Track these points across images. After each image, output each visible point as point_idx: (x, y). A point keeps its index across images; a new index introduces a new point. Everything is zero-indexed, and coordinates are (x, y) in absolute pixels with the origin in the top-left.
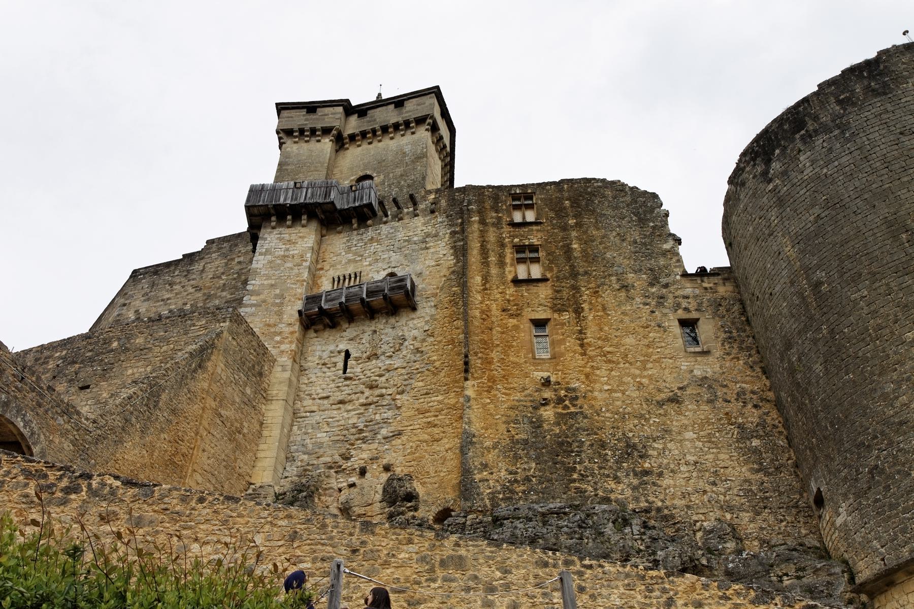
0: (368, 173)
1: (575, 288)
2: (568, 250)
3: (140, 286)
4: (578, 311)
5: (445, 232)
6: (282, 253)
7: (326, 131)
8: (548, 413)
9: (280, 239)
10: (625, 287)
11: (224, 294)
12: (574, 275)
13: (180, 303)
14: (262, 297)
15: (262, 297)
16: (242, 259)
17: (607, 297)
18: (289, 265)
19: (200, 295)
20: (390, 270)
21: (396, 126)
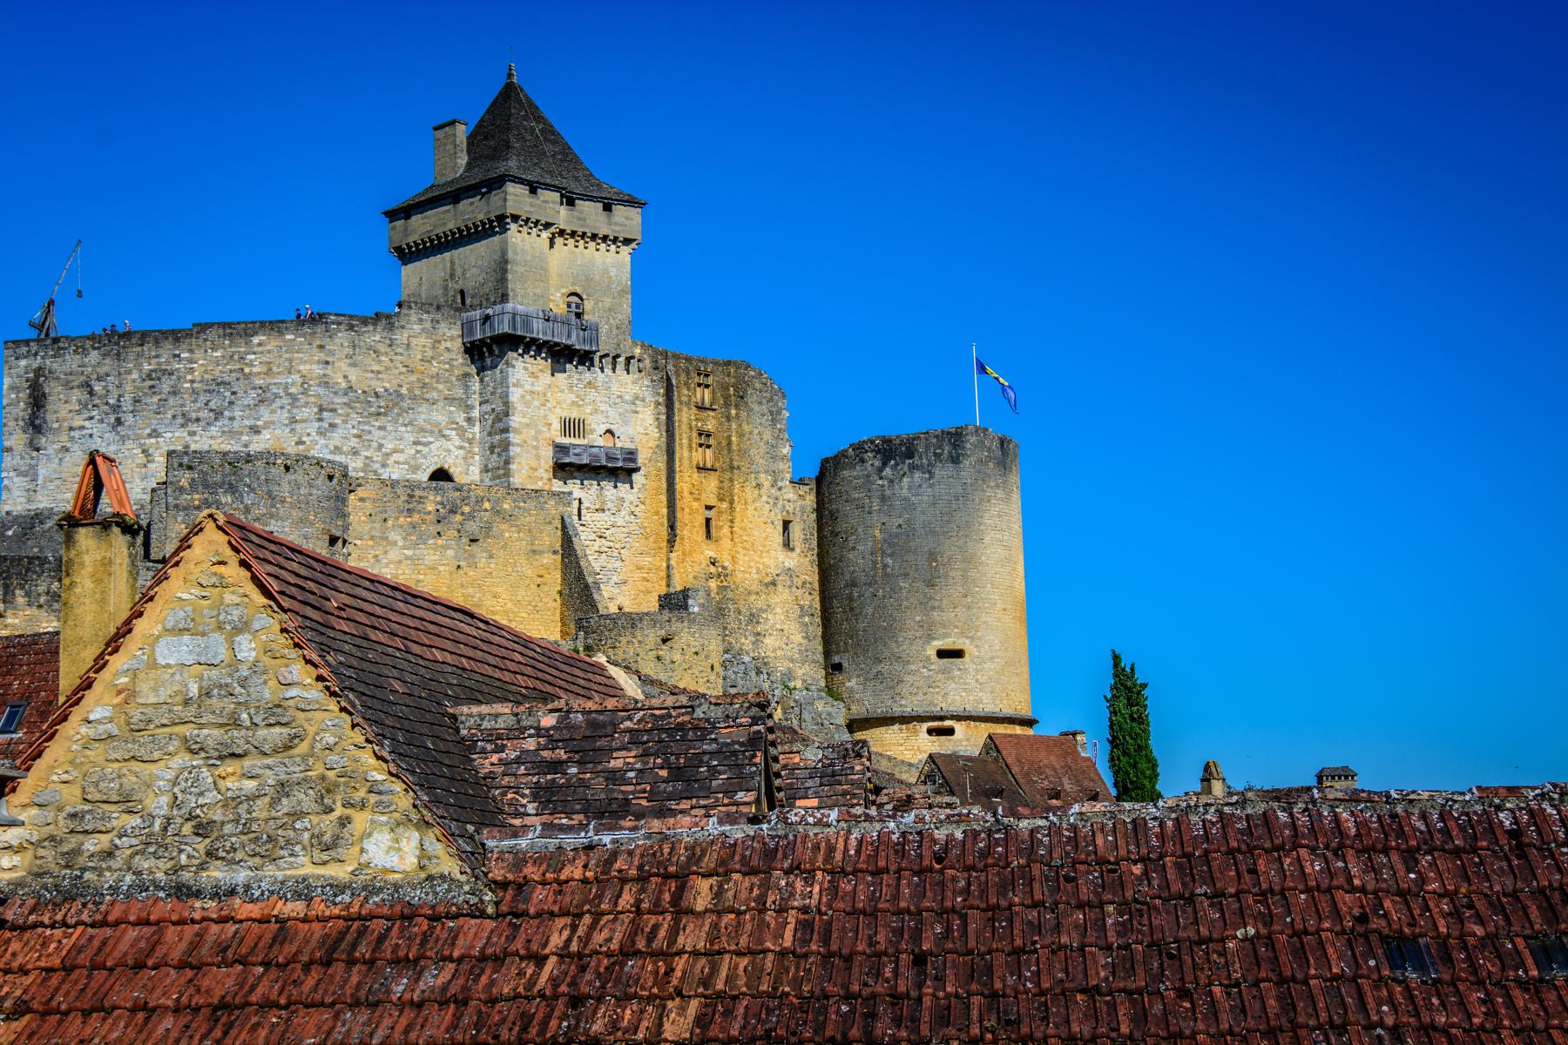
0: (579, 290)
1: (731, 480)
2: (729, 443)
3: (337, 341)
4: (732, 502)
5: (650, 398)
6: (528, 387)
7: (547, 225)
8: (713, 584)
9: (526, 369)
10: (759, 486)
11: (441, 387)
12: (732, 468)
13: (395, 382)
14: (523, 437)
15: (523, 437)
16: (449, 344)
17: (750, 493)
18: (536, 403)
19: (413, 378)
20: (608, 426)
21: (605, 238)
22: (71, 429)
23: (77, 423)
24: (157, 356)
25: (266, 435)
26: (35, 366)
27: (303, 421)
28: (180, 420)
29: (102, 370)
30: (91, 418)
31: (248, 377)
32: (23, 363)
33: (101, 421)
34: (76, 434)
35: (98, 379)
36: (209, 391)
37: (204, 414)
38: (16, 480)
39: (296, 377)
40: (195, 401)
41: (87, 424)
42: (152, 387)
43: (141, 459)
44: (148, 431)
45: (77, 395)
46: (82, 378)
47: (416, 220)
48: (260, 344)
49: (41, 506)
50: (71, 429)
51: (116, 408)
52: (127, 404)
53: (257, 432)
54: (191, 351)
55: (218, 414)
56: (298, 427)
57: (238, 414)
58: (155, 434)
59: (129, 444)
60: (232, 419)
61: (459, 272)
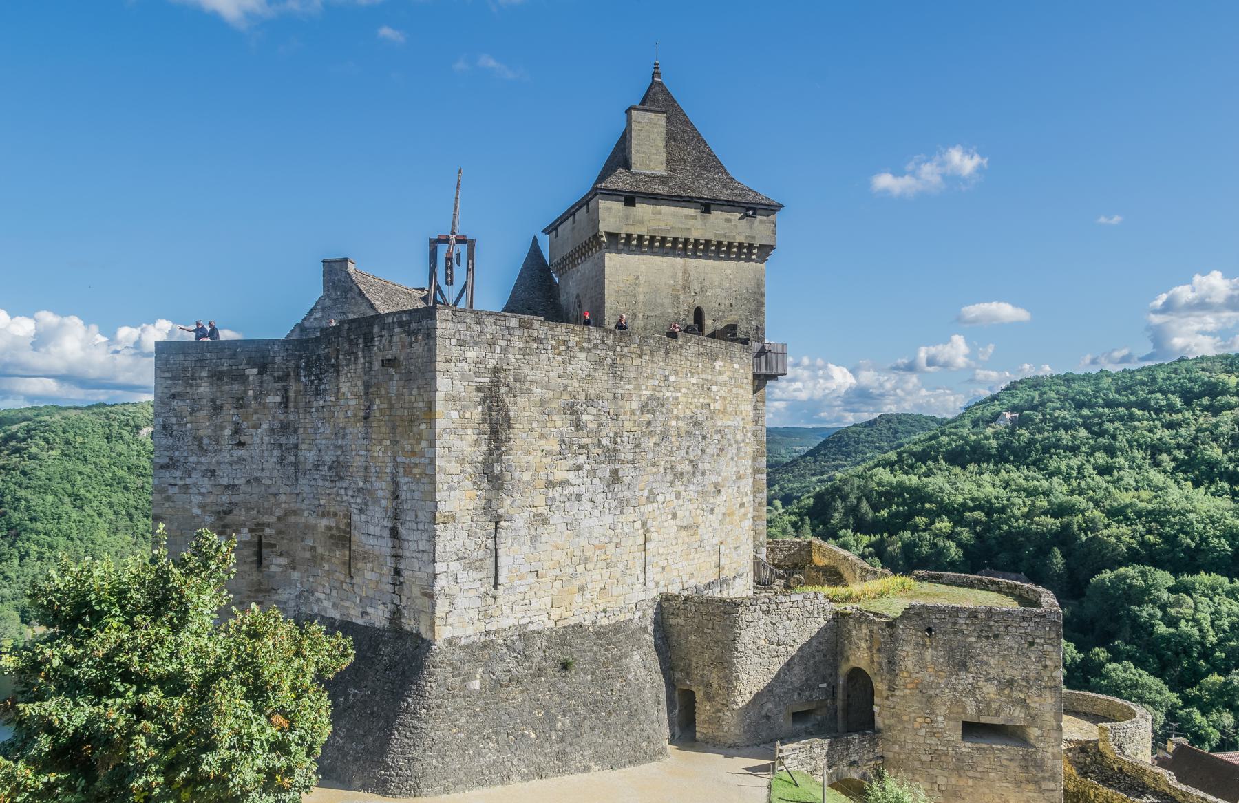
22: (549, 484)
23: (559, 475)
24: (653, 376)
25: (723, 497)
26: (492, 363)
27: (744, 477)
28: (669, 477)
29: (593, 389)
30: (579, 467)
31: (712, 415)
32: (472, 354)
33: (592, 473)
34: (556, 493)
35: (590, 403)
36: (689, 434)
37: (686, 467)
38: (463, 576)
39: (739, 419)
40: (679, 448)
41: (571, 476)
42: (649, 423)
43: (641, 540)
44: (646, 493)
45: (560, 424)
46: (566, 398)
47: (642, 209)
48: (720, 373)
49: (505, 623)
50: (549, 484)
51: (611, 454)
52: (626, 452)
53: (719, 491)
54: (676, 373)
55: (696, 466)
56: (741, 483)
57: (707, 466)
58: (651, 499)
59: (630, 514)
60: (703, 473)
61: (696, 286)
